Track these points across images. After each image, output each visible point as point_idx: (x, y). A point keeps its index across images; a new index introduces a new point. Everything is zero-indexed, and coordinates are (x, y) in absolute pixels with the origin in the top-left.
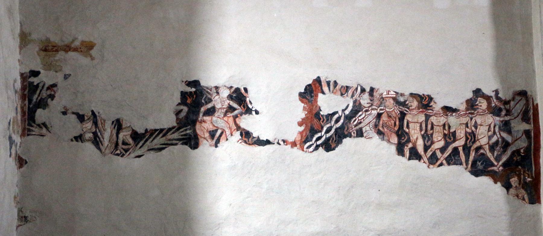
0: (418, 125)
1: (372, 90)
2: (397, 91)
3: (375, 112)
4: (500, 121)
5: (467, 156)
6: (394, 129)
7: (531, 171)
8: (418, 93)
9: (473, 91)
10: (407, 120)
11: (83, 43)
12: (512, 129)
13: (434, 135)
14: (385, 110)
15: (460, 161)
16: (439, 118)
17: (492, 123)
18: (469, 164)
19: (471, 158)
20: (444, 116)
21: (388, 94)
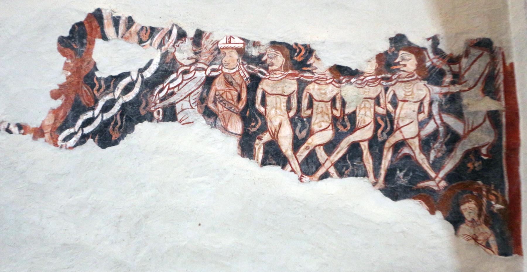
0: (284, 99)
1: (199, 34)
2: (247, 38)
3: (201, 76)
4: (442, 94)
5: (378, 159)
6: (237, 107)
7: (503, 191)
8: (286, 42)
9: (391, 39)
10: (262, 90)
12: (464, 109)
13: (313, 120)
14: (220, 71)
15: (364, 169)
16: (324, 87)
17: (425, 97)
18: (381, 174)
19: (385, 163)
20: (333, 83)
21: (230, 43)
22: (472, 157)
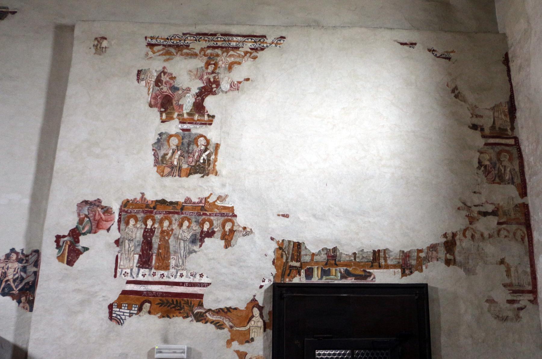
22: (27, 284)
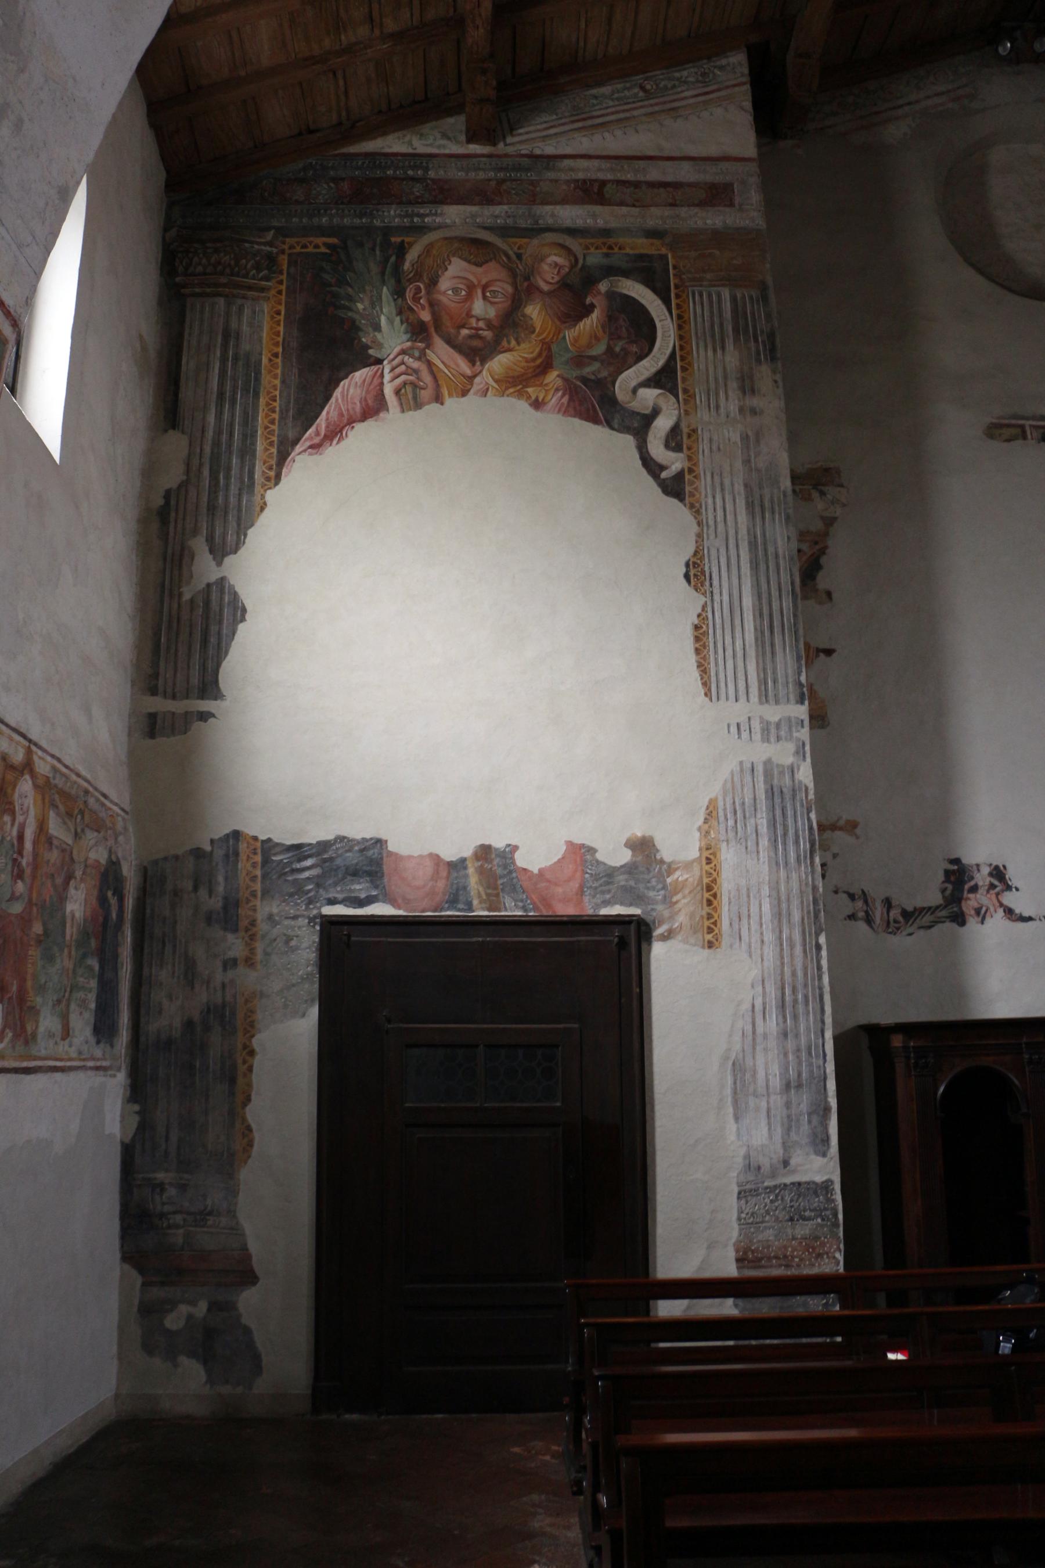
11: (848, 822)
